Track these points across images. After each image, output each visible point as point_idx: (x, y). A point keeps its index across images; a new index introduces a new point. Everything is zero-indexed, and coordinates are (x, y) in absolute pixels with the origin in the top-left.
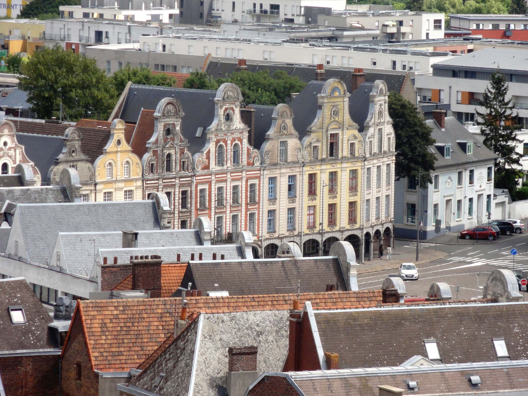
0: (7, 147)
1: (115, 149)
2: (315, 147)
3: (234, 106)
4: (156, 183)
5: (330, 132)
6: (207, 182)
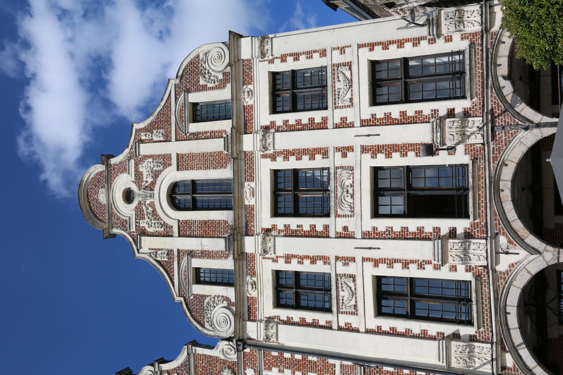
0: (134, 188)
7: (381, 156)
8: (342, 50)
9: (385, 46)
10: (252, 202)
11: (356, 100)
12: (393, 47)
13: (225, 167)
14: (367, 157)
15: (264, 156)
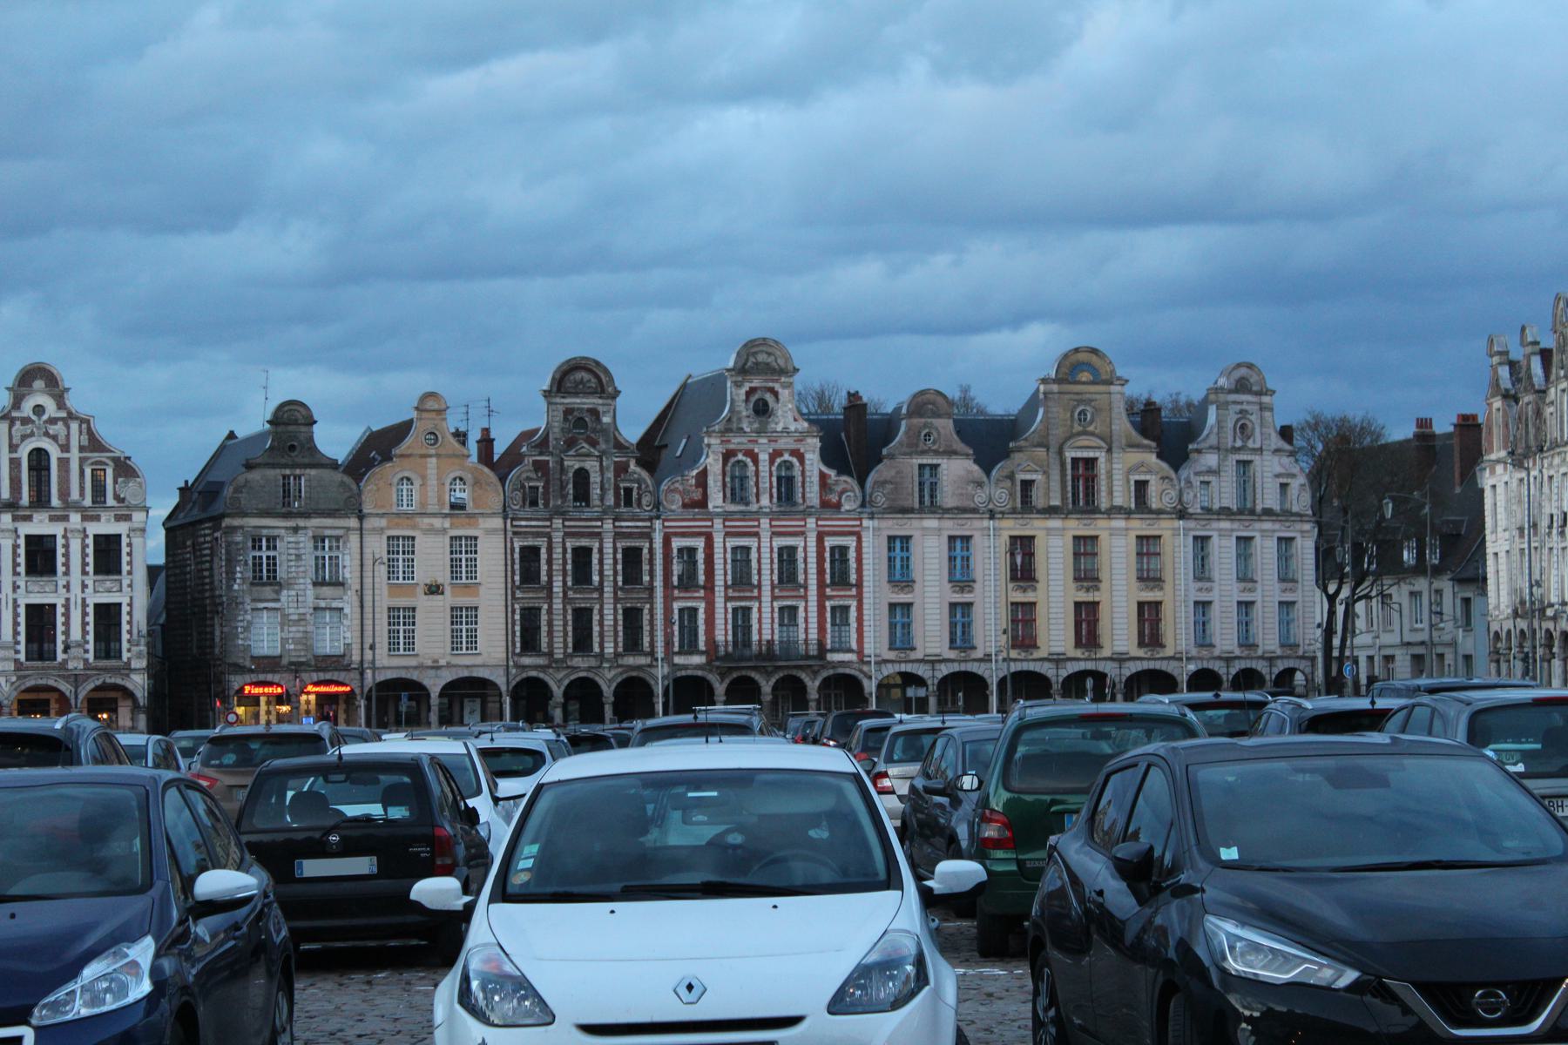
0: (45, 417)
1: (424, 451)
2: (1027, 485)
3: (777, 387)
4: (547, 527)
5: (1069, 454)
6: (699, 534)
7: (63, 610)
8: (130, 586)
9: (130, 613)
10: (34, 520)
11: (98, 594)
12: (128, 618)
13: (59, 499)
14: (64, 602)
15: (66, 530)
